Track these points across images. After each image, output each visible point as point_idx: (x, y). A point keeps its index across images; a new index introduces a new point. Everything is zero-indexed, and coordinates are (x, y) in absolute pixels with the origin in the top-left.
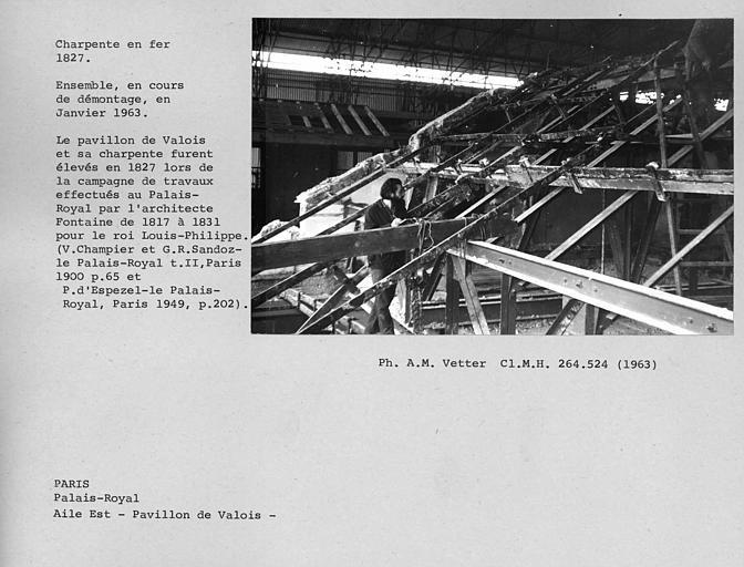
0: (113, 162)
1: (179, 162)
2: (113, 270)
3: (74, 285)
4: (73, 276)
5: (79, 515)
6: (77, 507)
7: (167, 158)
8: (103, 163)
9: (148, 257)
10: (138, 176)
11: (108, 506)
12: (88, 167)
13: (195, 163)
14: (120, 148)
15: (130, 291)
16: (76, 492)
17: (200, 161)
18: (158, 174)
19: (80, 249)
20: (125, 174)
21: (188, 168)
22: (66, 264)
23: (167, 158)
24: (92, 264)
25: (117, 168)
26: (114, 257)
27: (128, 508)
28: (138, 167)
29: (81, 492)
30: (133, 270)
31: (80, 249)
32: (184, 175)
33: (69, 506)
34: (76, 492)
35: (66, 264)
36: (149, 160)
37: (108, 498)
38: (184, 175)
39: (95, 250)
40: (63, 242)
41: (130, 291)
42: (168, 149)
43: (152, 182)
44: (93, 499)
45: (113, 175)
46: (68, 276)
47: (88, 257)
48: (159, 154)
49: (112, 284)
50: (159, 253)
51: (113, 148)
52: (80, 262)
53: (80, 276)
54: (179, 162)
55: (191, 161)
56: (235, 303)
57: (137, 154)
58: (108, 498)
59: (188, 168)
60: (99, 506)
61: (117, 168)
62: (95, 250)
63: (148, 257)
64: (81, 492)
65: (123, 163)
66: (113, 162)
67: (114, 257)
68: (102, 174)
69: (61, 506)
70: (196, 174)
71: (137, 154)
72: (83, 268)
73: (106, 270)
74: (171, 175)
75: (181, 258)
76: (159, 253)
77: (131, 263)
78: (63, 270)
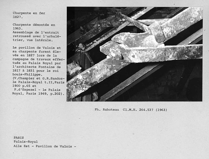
0: (23, 54)
1: (41, 54)
2: (28, 84)
3: (17, 88)
4: (17, 86)
5: (21, 146)
6: (20, 144)
7: (38, 53)
8: (20, 54)
9: (38, 80)
10: (30, 58)
11: (29, 144)
12: (15, 55)
13: (46, 54)
14: (24, 50)
15: (33, 90)
16: (20, 140)
17: (47, 54)
18: (35, 57)
19: (19, 78)
20: (26, 57)
21: (44, 56)
22: (15, 82)
23: (38, 53)
24: (23, 82)
25: (24, 55)
26: (29, 80)
27: (35, 144)
28: (30, 55)
29: (21, 140)
30: (34, 84)
31: (19, 78)
32: (42, 58)
33: (18, 144)
34: (20, 140)
35: (15, 82)
36: (33, 53)
37: (29, 141)
38: (42, 58)
39: (24, 79)
40: (15, 76)
41: (33, 90)
42: (38, 50)
43: (34, 59)
44: (25, 142)
45: (23, 57)
46: (16, 86)
47: (22, 80)
48: (36, 52)
49: (28, 88)
50: (41, 79)
51: (23, 50)
52: (19, 82)
53: (19, 86)
54: (41, 54)
55: (45, 54)
56: (61, 93)
57: (29, 52)
58: (29, 141)
59: (44, 56)
60: (27, 144)
61: (24, 55)
62: (24, 79)
63: (38, 80)
64: (21, 140)
65: (25, 54)
66: (23, 54)
67: (29, 80)
68: (19, 57)
69: (16, 144)
70: (46, 57)
71: (29, 52)
72: (20, 84)
73: (27, 84)
74: (39, 58)
75: (47, 81)
76: (41, 79)
77: (33, 82)
78: (14, 84)
